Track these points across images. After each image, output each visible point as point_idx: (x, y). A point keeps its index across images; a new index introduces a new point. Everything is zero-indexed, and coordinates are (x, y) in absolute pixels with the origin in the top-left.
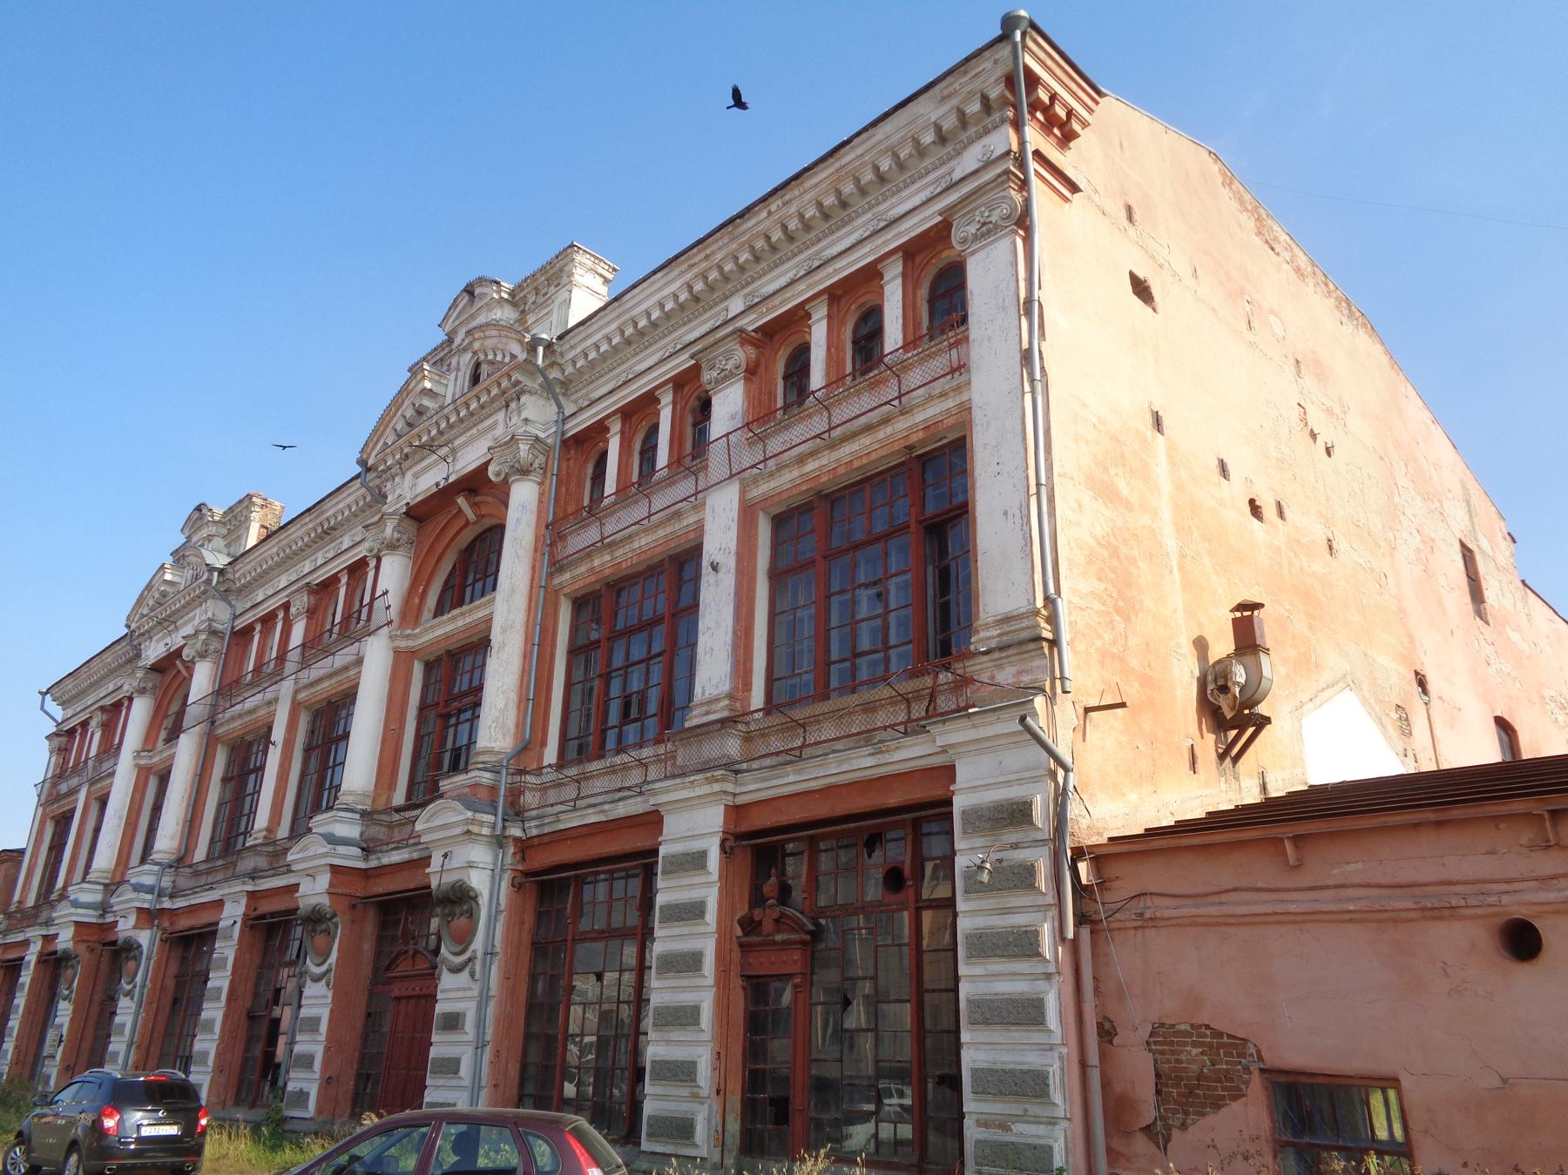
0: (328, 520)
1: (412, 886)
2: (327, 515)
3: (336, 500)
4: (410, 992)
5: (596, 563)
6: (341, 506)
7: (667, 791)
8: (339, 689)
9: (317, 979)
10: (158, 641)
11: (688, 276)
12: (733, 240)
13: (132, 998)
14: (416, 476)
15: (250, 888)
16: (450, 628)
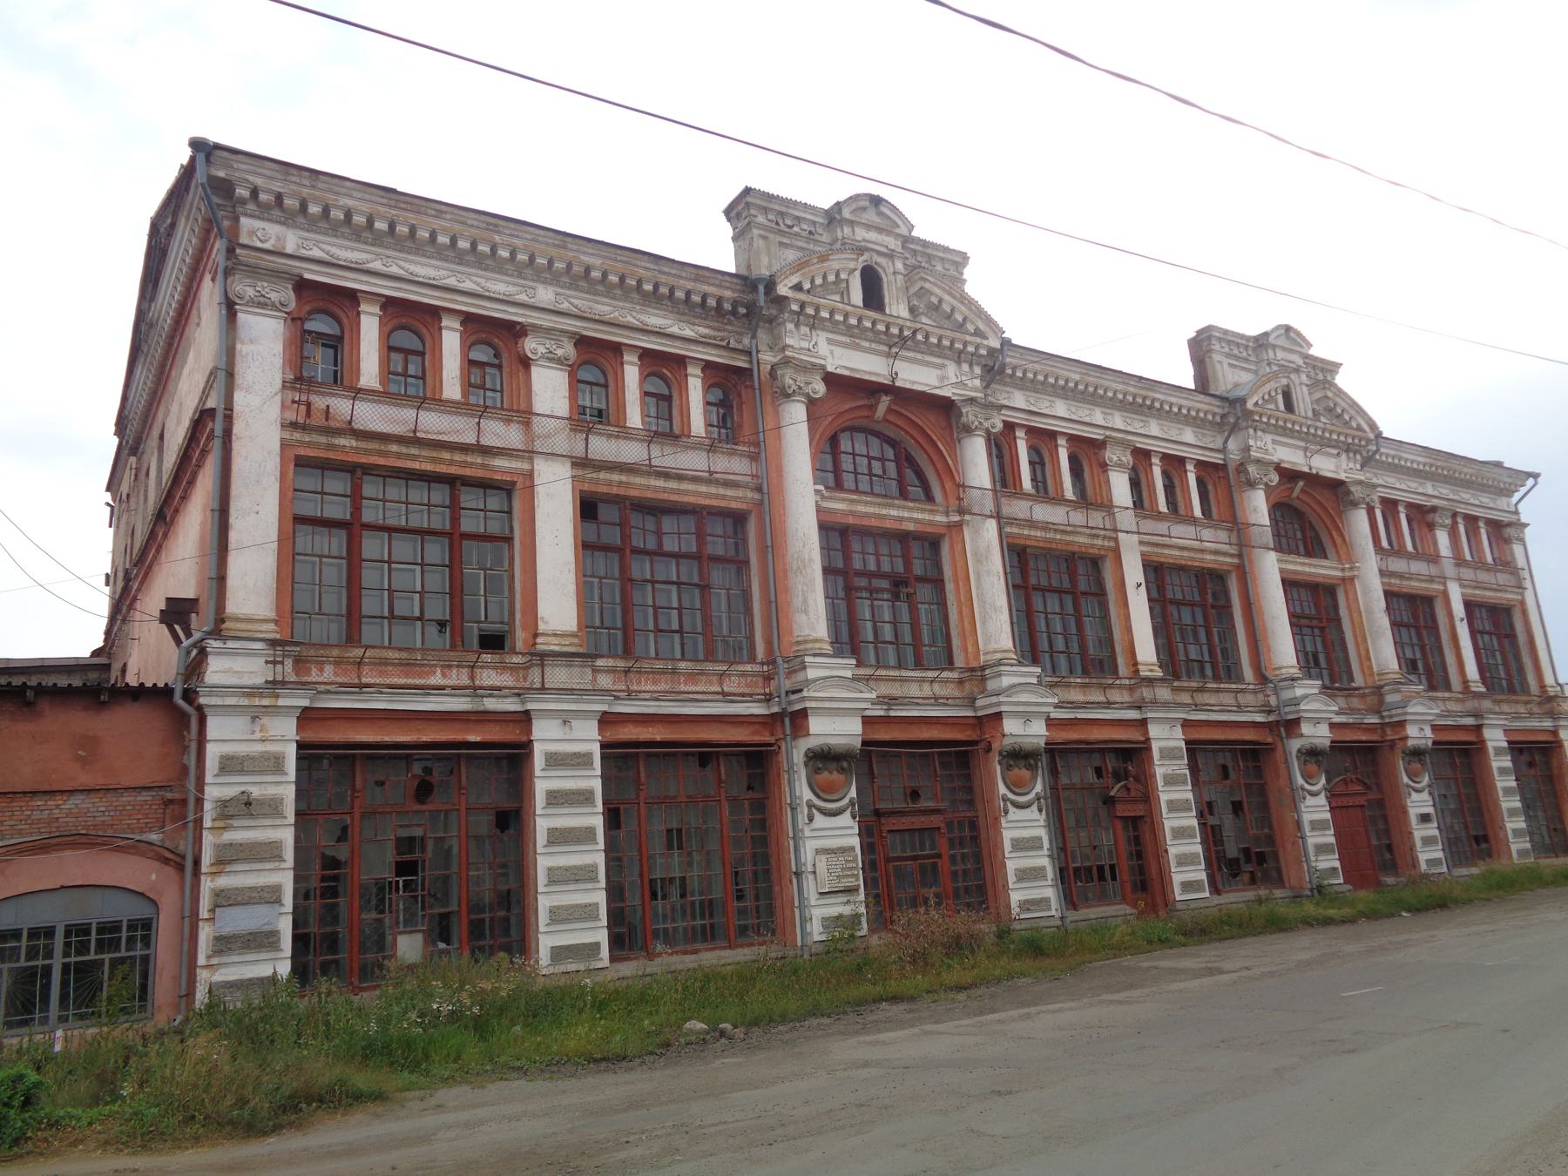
0: (1153, 400)
1: (1348, 739)
2: (1157, 396)
3: (1168, 392)
4: (1345, 804)
5: (1393, 581)
6: (1174, 400)
7: (1492, 719)
8: (1189, 563)
9: (1314, 794)
10: (830, 342)
11: (1427, 460)
12: (1446, 461)
13: (1040, 810)
14: (1274, 442)
15: (1184, 716)
16: (1299, 568)
